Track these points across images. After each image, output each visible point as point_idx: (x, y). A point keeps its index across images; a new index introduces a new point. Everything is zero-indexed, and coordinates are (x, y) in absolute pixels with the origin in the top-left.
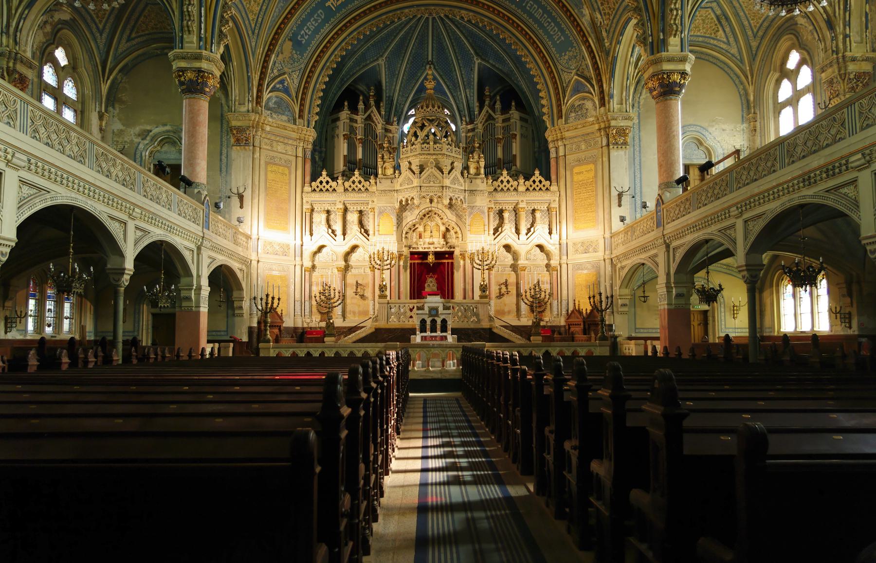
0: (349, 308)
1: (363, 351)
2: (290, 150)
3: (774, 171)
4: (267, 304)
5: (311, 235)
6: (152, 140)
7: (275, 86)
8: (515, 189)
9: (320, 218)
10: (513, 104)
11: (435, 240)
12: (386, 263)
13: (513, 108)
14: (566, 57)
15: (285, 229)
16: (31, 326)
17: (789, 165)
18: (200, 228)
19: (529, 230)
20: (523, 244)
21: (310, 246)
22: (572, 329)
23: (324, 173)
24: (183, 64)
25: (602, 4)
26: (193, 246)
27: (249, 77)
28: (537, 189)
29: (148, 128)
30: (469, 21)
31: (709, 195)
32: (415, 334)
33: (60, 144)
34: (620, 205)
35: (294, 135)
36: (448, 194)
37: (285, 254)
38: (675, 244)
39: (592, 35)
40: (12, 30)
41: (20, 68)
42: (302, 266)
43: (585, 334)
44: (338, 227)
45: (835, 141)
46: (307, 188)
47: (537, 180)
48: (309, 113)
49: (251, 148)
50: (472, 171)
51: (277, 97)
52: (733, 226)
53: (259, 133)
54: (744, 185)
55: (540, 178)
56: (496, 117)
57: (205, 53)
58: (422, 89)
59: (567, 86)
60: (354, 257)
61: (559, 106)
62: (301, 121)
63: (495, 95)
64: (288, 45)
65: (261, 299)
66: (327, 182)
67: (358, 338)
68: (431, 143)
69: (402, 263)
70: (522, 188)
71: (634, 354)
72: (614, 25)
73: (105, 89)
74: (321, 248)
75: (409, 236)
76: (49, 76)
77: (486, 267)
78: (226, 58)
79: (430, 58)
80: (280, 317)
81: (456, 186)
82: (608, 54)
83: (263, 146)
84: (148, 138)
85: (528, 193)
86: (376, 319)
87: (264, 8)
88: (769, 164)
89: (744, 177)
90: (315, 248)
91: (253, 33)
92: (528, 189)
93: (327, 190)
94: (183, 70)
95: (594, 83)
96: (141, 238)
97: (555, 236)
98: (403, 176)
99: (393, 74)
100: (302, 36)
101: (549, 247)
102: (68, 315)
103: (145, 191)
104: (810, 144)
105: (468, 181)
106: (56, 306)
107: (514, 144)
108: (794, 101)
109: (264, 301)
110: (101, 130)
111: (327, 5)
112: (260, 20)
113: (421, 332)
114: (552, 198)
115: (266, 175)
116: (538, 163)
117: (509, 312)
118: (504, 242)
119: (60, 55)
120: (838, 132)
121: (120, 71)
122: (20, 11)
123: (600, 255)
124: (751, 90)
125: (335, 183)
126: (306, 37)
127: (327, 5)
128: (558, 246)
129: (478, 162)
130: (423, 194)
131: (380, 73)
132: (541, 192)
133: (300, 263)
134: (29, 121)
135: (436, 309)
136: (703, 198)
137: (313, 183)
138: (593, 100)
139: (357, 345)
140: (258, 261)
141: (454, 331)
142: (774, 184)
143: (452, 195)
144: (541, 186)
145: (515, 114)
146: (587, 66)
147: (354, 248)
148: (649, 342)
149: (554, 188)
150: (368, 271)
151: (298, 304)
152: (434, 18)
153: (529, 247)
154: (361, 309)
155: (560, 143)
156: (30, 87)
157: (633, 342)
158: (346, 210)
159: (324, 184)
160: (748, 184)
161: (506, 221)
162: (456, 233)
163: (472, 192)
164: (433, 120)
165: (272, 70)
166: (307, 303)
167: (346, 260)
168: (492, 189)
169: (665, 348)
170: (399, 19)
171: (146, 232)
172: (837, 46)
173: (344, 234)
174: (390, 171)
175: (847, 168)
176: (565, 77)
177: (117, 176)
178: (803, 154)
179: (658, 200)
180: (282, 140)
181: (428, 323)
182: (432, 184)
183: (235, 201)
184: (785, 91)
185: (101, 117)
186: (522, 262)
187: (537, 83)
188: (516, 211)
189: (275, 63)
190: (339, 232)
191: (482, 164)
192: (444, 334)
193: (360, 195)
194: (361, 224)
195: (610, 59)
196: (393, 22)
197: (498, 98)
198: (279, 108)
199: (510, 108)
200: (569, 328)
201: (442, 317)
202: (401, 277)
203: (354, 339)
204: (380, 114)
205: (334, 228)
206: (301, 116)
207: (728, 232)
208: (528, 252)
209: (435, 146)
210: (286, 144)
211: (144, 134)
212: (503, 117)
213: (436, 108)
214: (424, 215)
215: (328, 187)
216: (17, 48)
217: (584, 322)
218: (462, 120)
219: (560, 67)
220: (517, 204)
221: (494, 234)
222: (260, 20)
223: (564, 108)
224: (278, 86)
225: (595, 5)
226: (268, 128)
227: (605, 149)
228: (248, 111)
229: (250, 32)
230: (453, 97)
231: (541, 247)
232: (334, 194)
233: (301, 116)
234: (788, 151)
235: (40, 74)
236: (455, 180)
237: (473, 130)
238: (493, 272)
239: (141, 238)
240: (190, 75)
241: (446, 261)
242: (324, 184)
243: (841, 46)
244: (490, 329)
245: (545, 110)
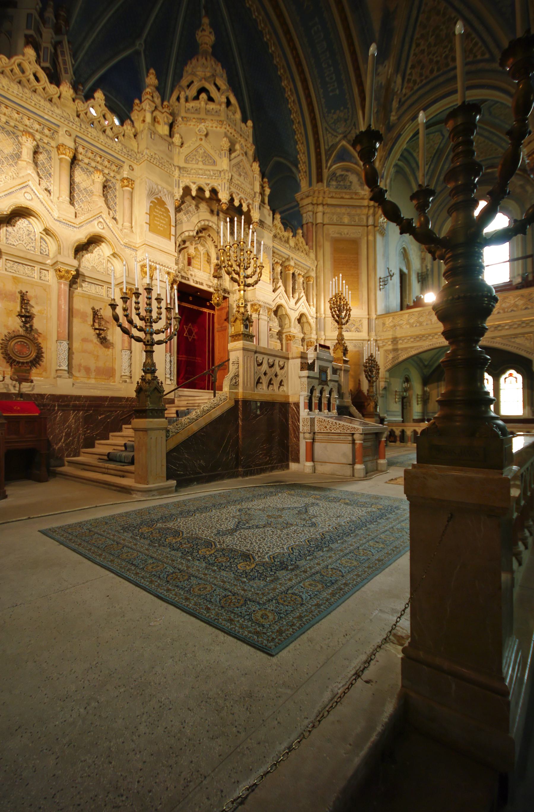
14: (335, 117)
25: (413, 67)
72: (415, 98)
147: (94, 241)
154: (101, 364)
220: (288, 259)
225: (403, 64)
241: (205, 310)
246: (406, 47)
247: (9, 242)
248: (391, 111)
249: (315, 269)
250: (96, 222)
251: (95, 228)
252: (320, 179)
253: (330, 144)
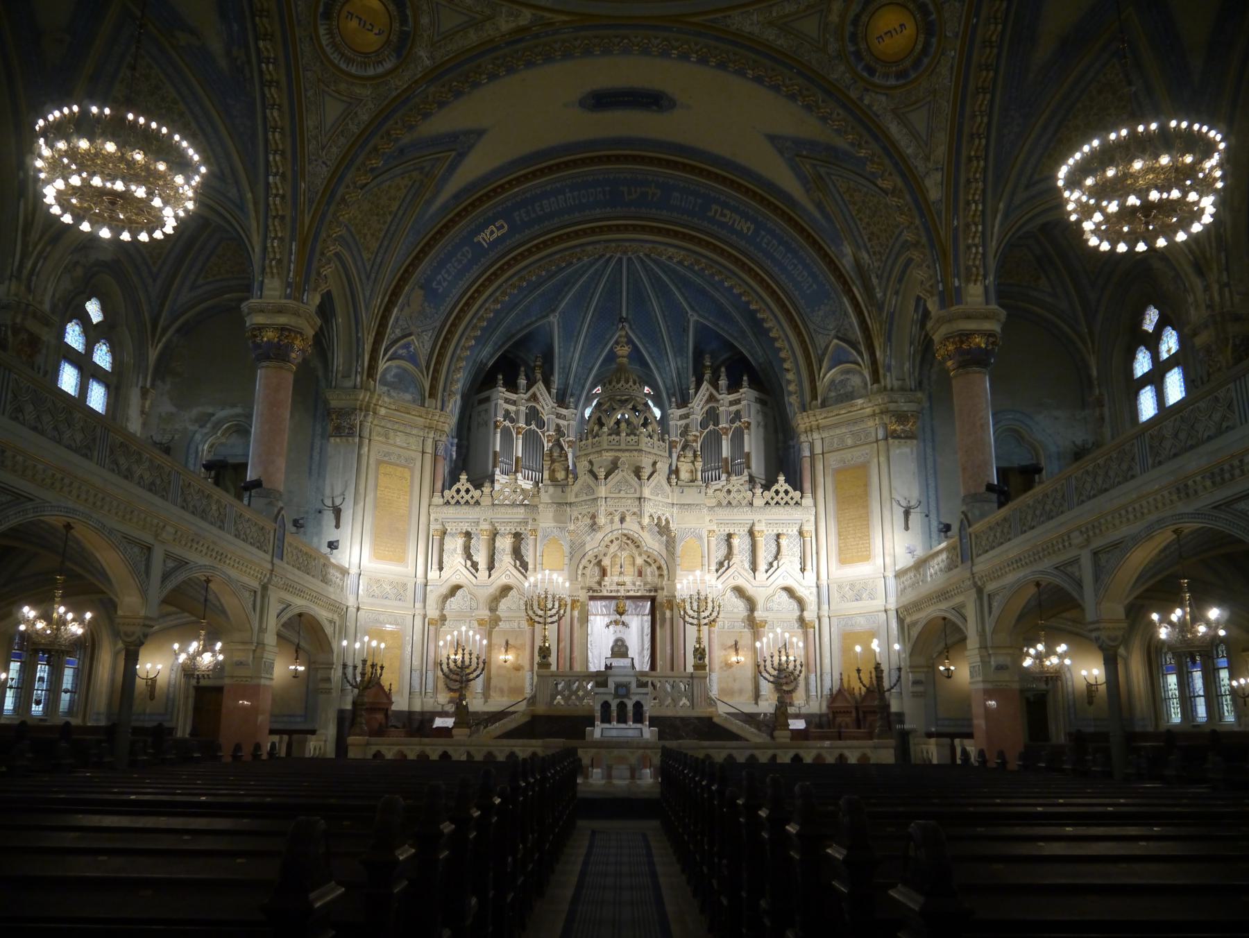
0: (493, 682)
1: (507, 751)
2: (415, 444)
3: (1133, 477)
4: (363, 674)
5: (441, 569)
6: (214, 428)
7: (395, 352)
8: (751, 504)
9: (455, 545)
10: (745, 378)
11: (628, 579)
12: (549, 613)
13: (745, 383)
14: (821, 313)
15: (401, 560)
16: (9, 704)
17: (1154, 466)
18: (268, 557)
19: (771, 565)
20: (763, 586)
21: (439, 581)
22: (839, 720)
23: (464, 477)
24: (260, 319)
25: (870, 240)
26: (255, 584)
27: (358, 339)
28: (782, 502)
29: (211, 410)
30: (680, 263)
31: (1038, 513)
32: (593, 725)
33: (56, 428)
34: (907, 528)
35: (420, 421)
36: (648, 509)
37: (399, 597)
38: (991, 587)
39: (858, 282)
40: (26, 272)
41: (31, 325)
42: (425, 616)
43: (859, 727)
44: (481, 558)
45: (1220, 432)
46: (437, 500)
47: (782, 490)
48: (444, 390)
49: (357, 440)
50: (684, 475)
51: (398, 367)
52: (1075, 561)
53: (370, 419)
54: (1089, 498)
55: (787, 486)
56: (720, 397)
57: (290, 303)
58: (612, 357)
59: (824, 354)
60: (504, 604)
61: (813, 381)
63: (719, 368)
64: (419, 293)
65: (355, 667)
66: (467, 491)
67: (504, 730)
68: (623, 434)
69: (576, 613)
70: (759, 502)
71: (935, 761)
73: (153, 355)
74: (455, 589)
75: (588, 572)
76: (74, 336)
77: (706, 621)
78: (326, 310)
79: (624, 315)
80: (388, 696)
81: (659, 498)
82: (880, 308)
83: (375, 437)
84: (209, 425)
85: (768, 508)
86: (532, 701)
87: (386, 243)
88: (1125, 466)
89: (1088, 486)
90: (444, 590)
91: (368, 278)
92: (767, 503)
93: (467, 502)
94: (261, 328)
95: (863, 349)
96: (175, 569)
97: (810, 575)
98: (579, 482)
99: (570, 335)
100: (439, 283)
101: (801, 592)
102: (69, 687)
103: (185, 500)
104: (1182, 436)
105: (677, 490)
106: (51, 674)
107: (746, 437)
108: (1156, 378)
109: (359, 670)
110: (143, 412)
111: (475, 240)
112: (379, 260)
113: (603, 721)
114: (805, 517)
115: (377, 478)
116: (784, 465)
117: (741, 691)
118: (733, 583)
119: (94, 309)
120: (1224, 418)
121: (178, 331)
122: (39, 247)
123: (879, 603)
124: (1093, 362)
125: (478, 492)
126: (445, 284)
127: (475, 240)
128: (814, 590)
129: (693, 462)
130: (611, 509)
131: (551, 332)
132: (787, 508)
133: (422, 612)
134: (10, 395)
135: (626, 686)
136: (1029, 518)
137: (446, 492)
138: (861, 374)
139: (505, 741)
140: (358, 609)
141: (654, 721)
142: (1134, 496)
144: (787, 498)
145: (747, 394)
146: (851, 325)
148: (957, 741)
149: (808, 501)
150: (525, 625)
151: (416, 675)
152: (629, 259)
153: (770, 591)
155: (816, 435)
156: (44, 351)
157: (933, 740)
158: (494, 535)
159: (463, 493)
160: (1095, 496)
161: (735, 551)
162: (659, 568)
164: (626, 401)
165: (393, 327)
166: (430, 674)
167: (493, 609)
168: (713, 502)
169: (981, 753)
170: (579, 259)
171: (182, 564)
172: (1211, 299)
173: (491, 567)
174: (560, 475)
175: (1242, 471)
176: (821, 341)
177: (141, 477)
178: (1173, 451)
179: (962, 522)
181: (614, 707)
182: (622, 494)
183: (329, 517)
184: (1143, 364)
185: (144, 393)
186: (758, 614)
187: (780, 349)
188: (751, 533)
189: (397, 319)
190: (483, 565)
191: (699, 465)
192: (639, 726)
193: (515, 510)
194: (517, 553)
195: (884, 315)
196: (570, 264)
197: (723, 369)
198: (401, 382)
199: (741, 386)
200: (834, 718)
201: (635, 699)
202: (576, 635)
203: (499, 733)
204: (550, 393)
205: (474, 558)
207: (1069, 569)
208: (768, 599)
209: (629, 439)
211: (202, 420)
212: (732, 397)
213: (631, 383)
214: (612, 542)
215: (468, 497)
216: (31, 298)
217: (857, 708)
218: (670, 402)
219: (811, 327)
220: (753, 524)
221: (717, 571)
222: (379, 260)
223: (822, 385)
224: (400, 352)
226: (383, 411)
227: (882, 443)
228: (355, 387)
229: (363, 277)
230: (658, 368)
231: (789, 591)
232: (477, 509)
233: (432, 395)
234: (1151, 447)
235: (62, 332)
237: (686, 416)
238: (716, 629)
239: (175, 569)
240: (269, 335)
242: (463, 493)
243: (1217, 297)
244: (710, 719)
245: (792, 388)
246: (853, 225)
248: (874, 289)
249: (813, 518)
251: (504, 580)
252: (814, 397)
253: (823, 346)
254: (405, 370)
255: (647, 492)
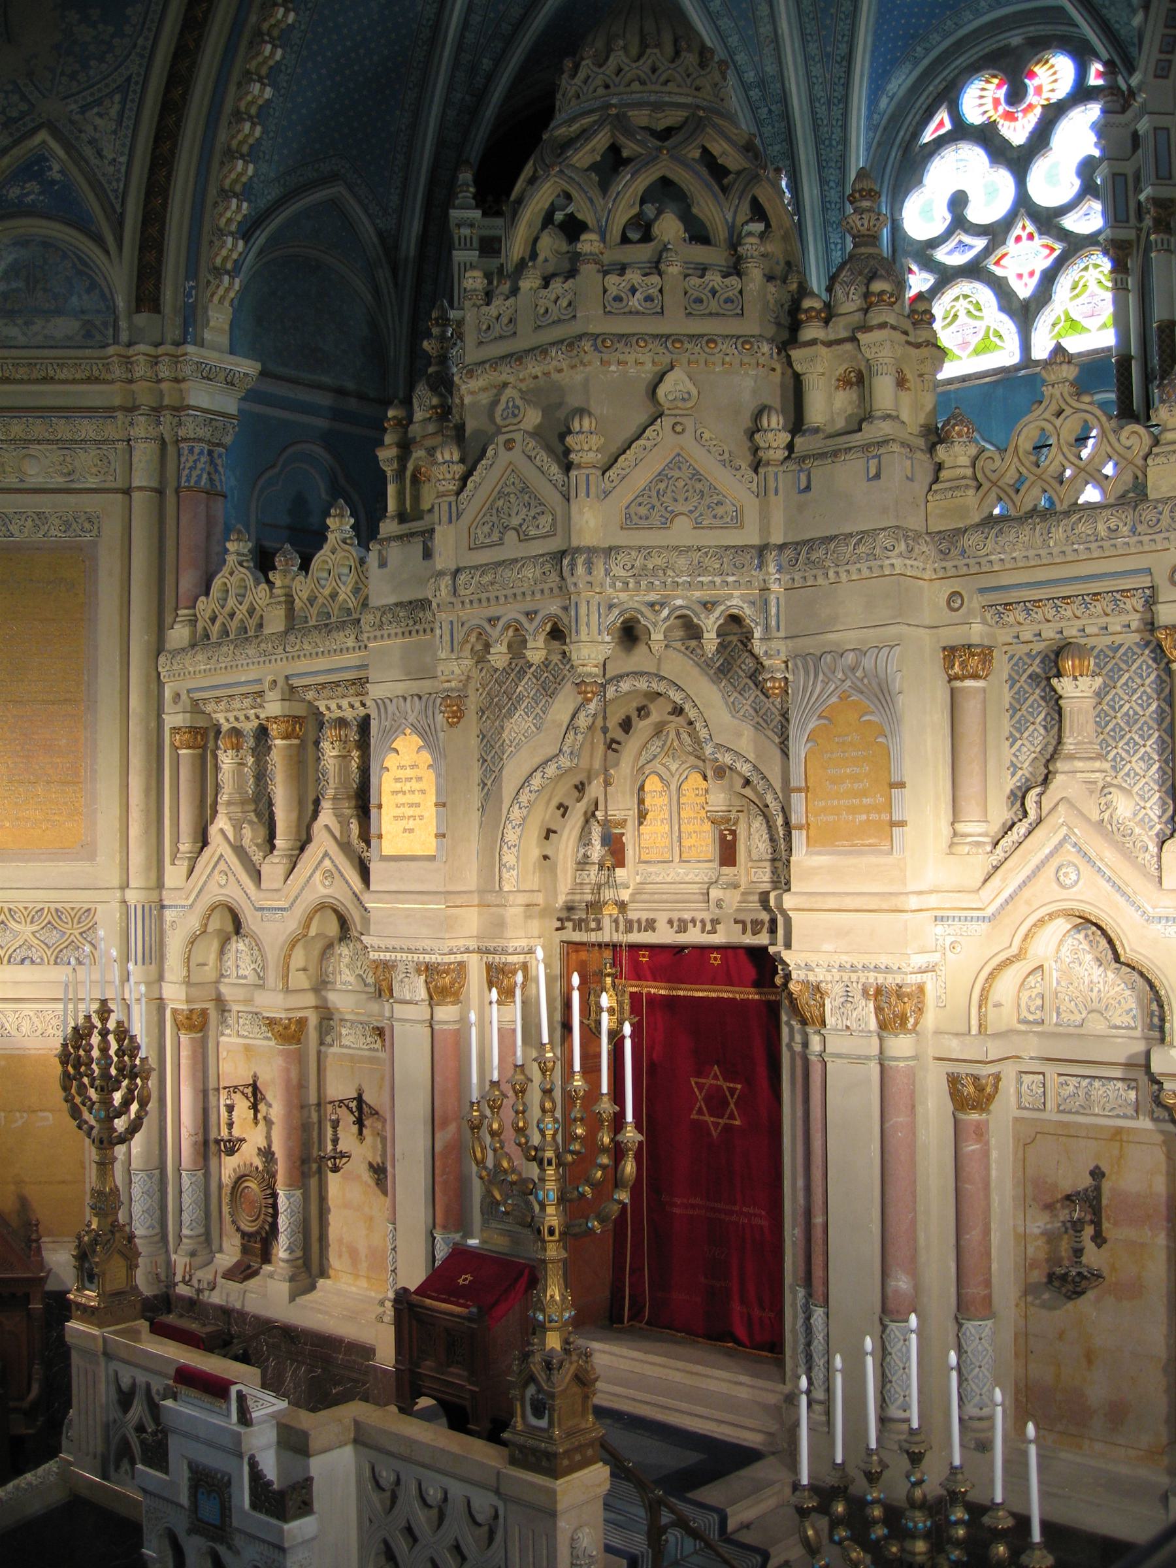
36: (599, 599)
42: (160, 1004)
51: (22, 242)
62: (141, 319)
81: (682, 532)
117: (1117, 1414)
143: (632, 599)
163: (803, 552)
180: (38, 429)
206: (147, 297)
210: (65, 444)
214: (626, 725)
233: (147, 297)
236: (679, 490)
247: (241, 972)
250: (318, 876)
254: (46, 244)
255: (591, 522)
